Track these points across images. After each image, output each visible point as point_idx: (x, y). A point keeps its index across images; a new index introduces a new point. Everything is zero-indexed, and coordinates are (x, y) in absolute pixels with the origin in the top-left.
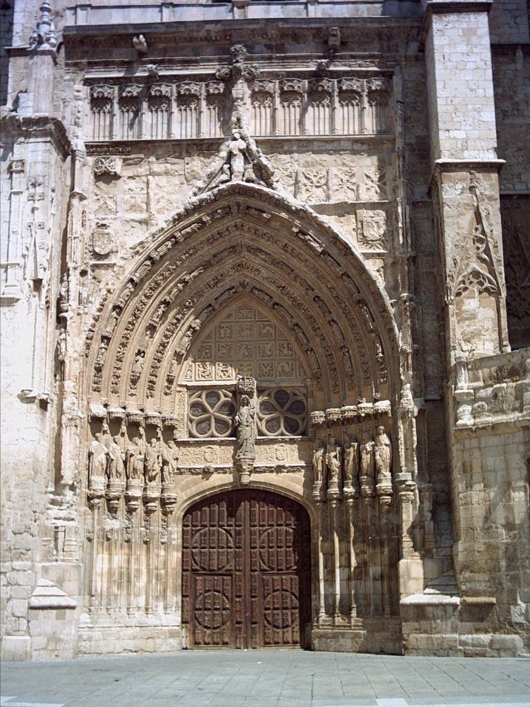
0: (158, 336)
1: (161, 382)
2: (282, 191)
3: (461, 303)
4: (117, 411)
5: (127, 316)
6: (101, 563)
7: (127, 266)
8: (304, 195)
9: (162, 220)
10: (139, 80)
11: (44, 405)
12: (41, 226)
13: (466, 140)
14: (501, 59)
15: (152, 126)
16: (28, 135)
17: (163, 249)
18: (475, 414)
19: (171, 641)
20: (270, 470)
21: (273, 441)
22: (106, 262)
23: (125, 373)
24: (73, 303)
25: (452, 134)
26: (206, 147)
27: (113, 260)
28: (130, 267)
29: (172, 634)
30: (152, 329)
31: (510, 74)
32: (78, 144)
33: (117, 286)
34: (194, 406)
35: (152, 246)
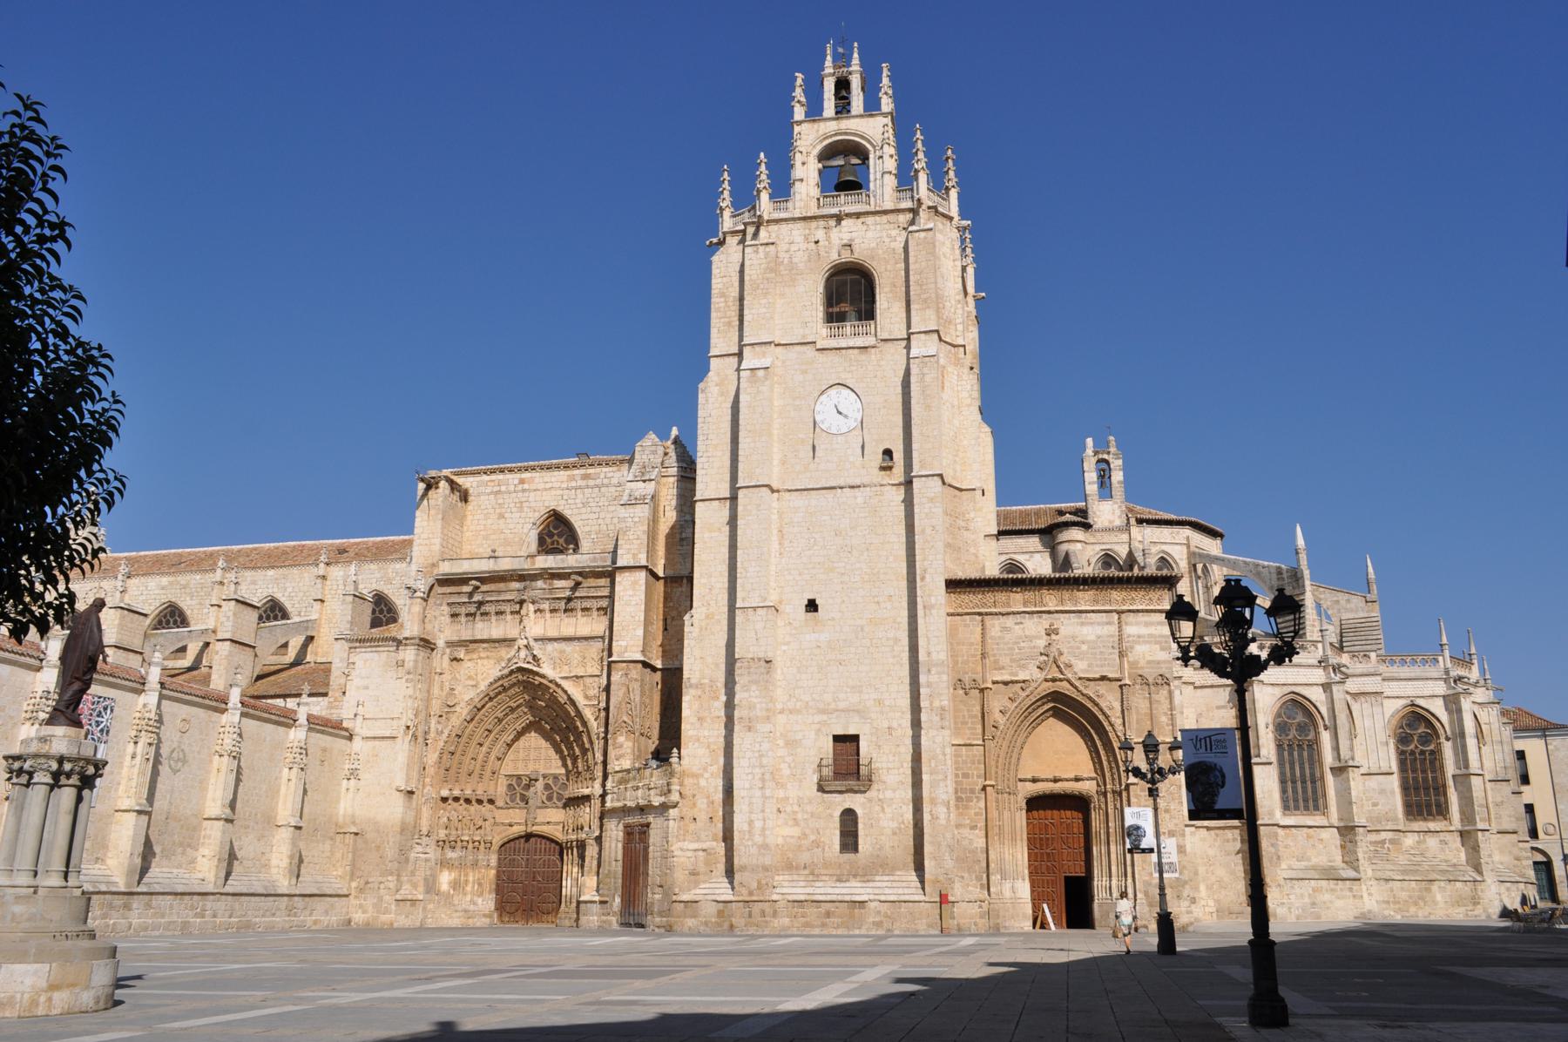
0: (484, 749)
1: (488, 773)
2: (547, 670)
3: (615, 739)
4: (456, 793)
5: (464, 740)
6: (445, 879)
7: (463, 711)
8: (558, 670)
9: (483, 686)
10: (475, 602)
11: (411, 793)
12: (410, 696)
13: (626, 647)
14: (674, 585)
15: (482, 629)
16: (406, 645)
17: (483, 702)
18: (612, 801)
19: (483, 920)
20: (544, 824)
21: (546, 807)
22: (453, 709)
23: (465, 770)
24: (432, 735)
25: (620, 643)
26: (507, 642)
27: (458, 709)
28: (465, 712)
29: (485, 916)
30: (481, 745)
31: (678, 594)
32: (440, 643)
33: (458, 723)
34: (510, 786)
35: (477, 700)
